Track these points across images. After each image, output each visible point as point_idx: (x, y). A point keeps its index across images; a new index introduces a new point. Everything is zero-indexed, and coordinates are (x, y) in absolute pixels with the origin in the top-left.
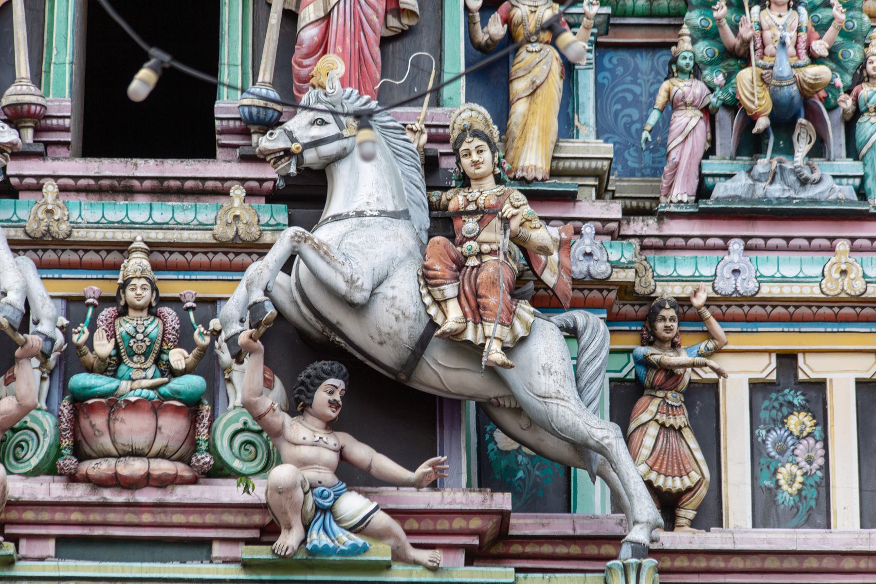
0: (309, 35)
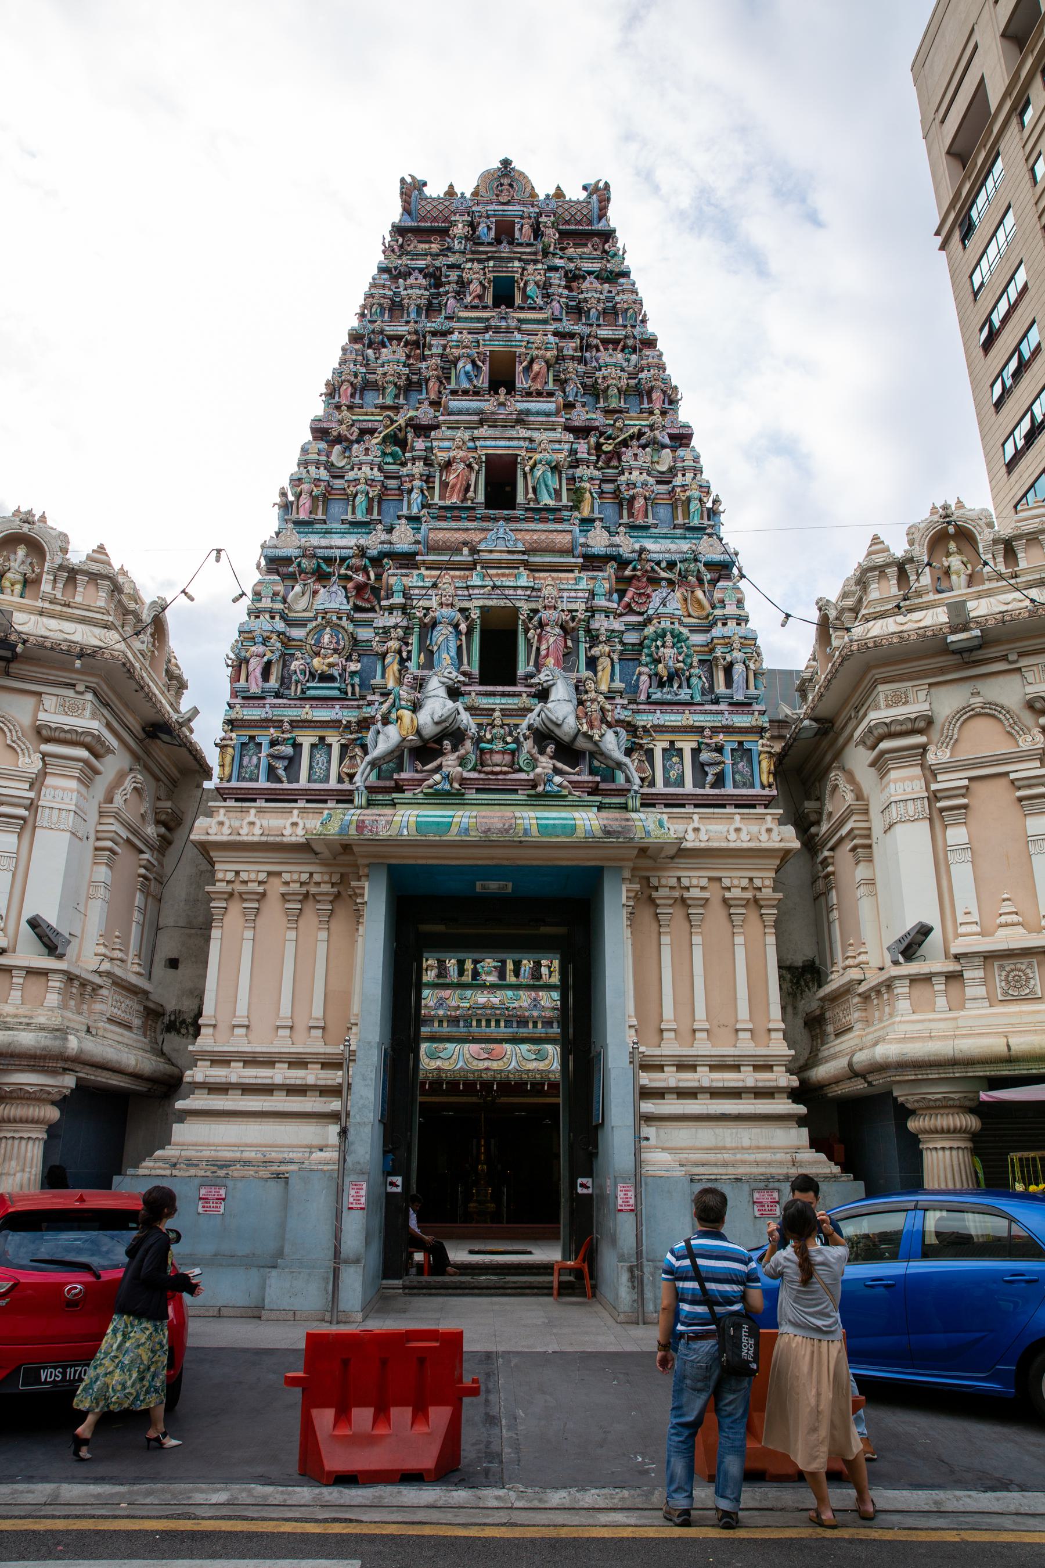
0: (543, 653)
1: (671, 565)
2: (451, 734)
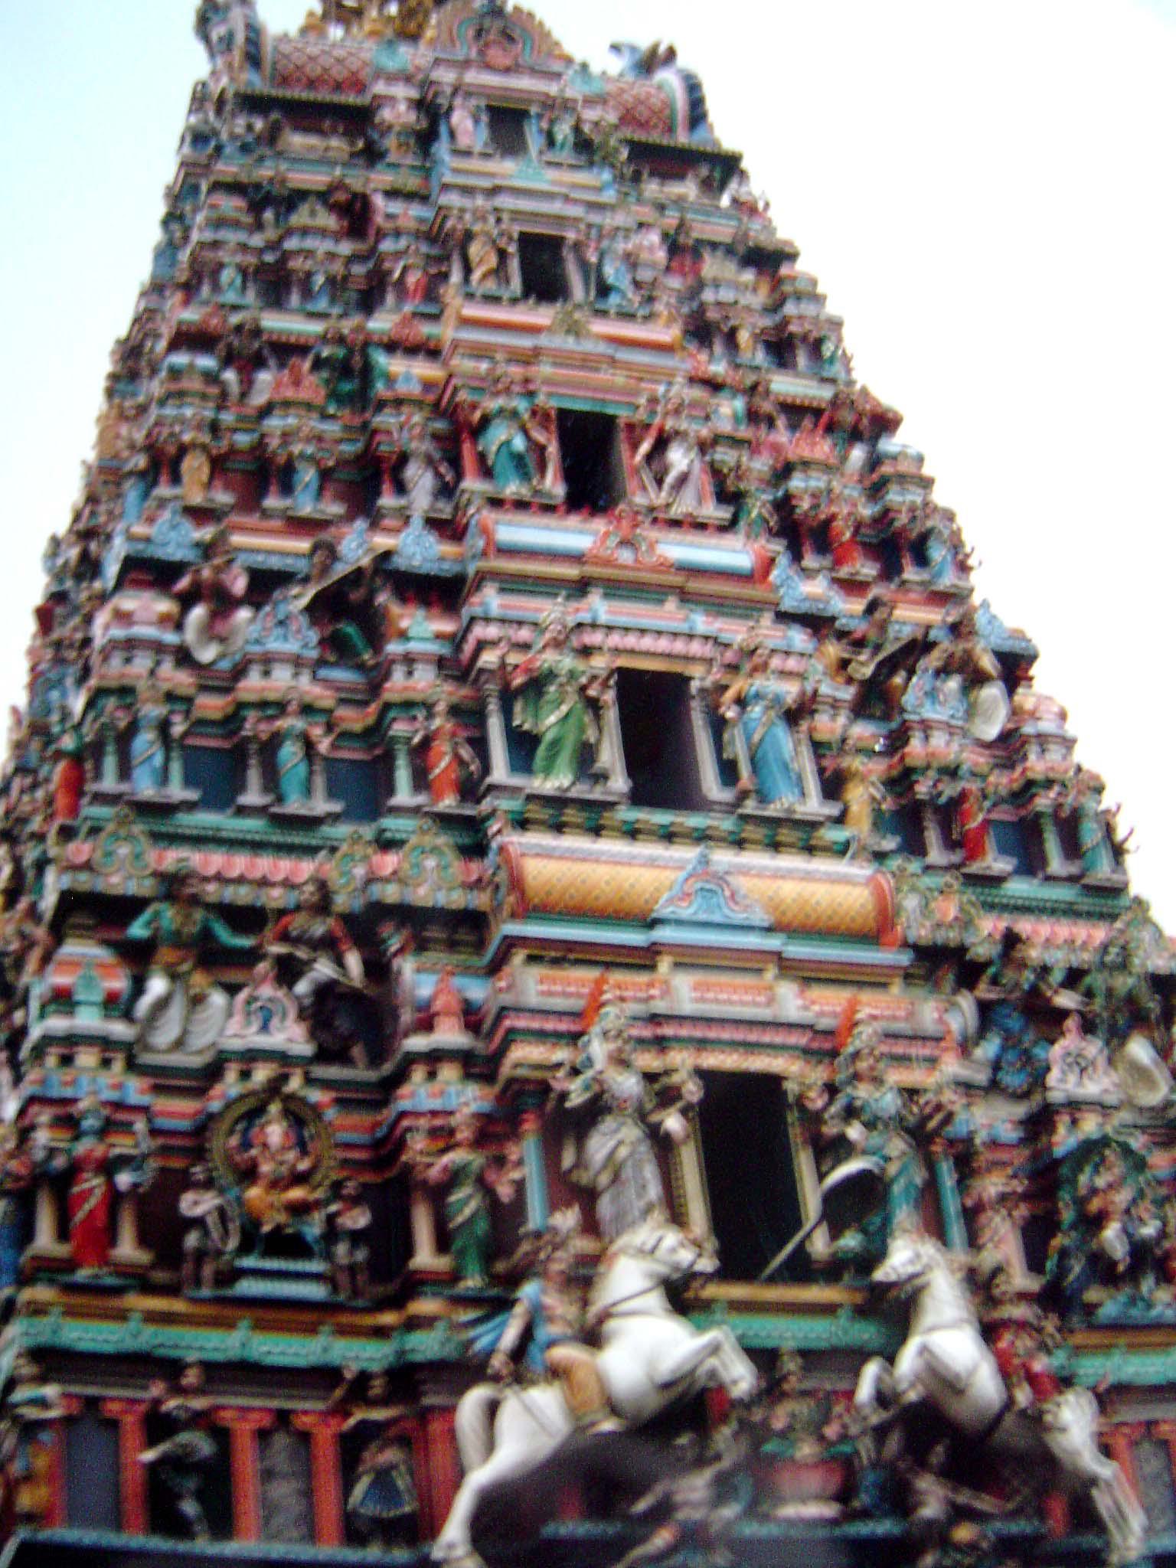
1: (1074, 977)
2: (686, 1410)
